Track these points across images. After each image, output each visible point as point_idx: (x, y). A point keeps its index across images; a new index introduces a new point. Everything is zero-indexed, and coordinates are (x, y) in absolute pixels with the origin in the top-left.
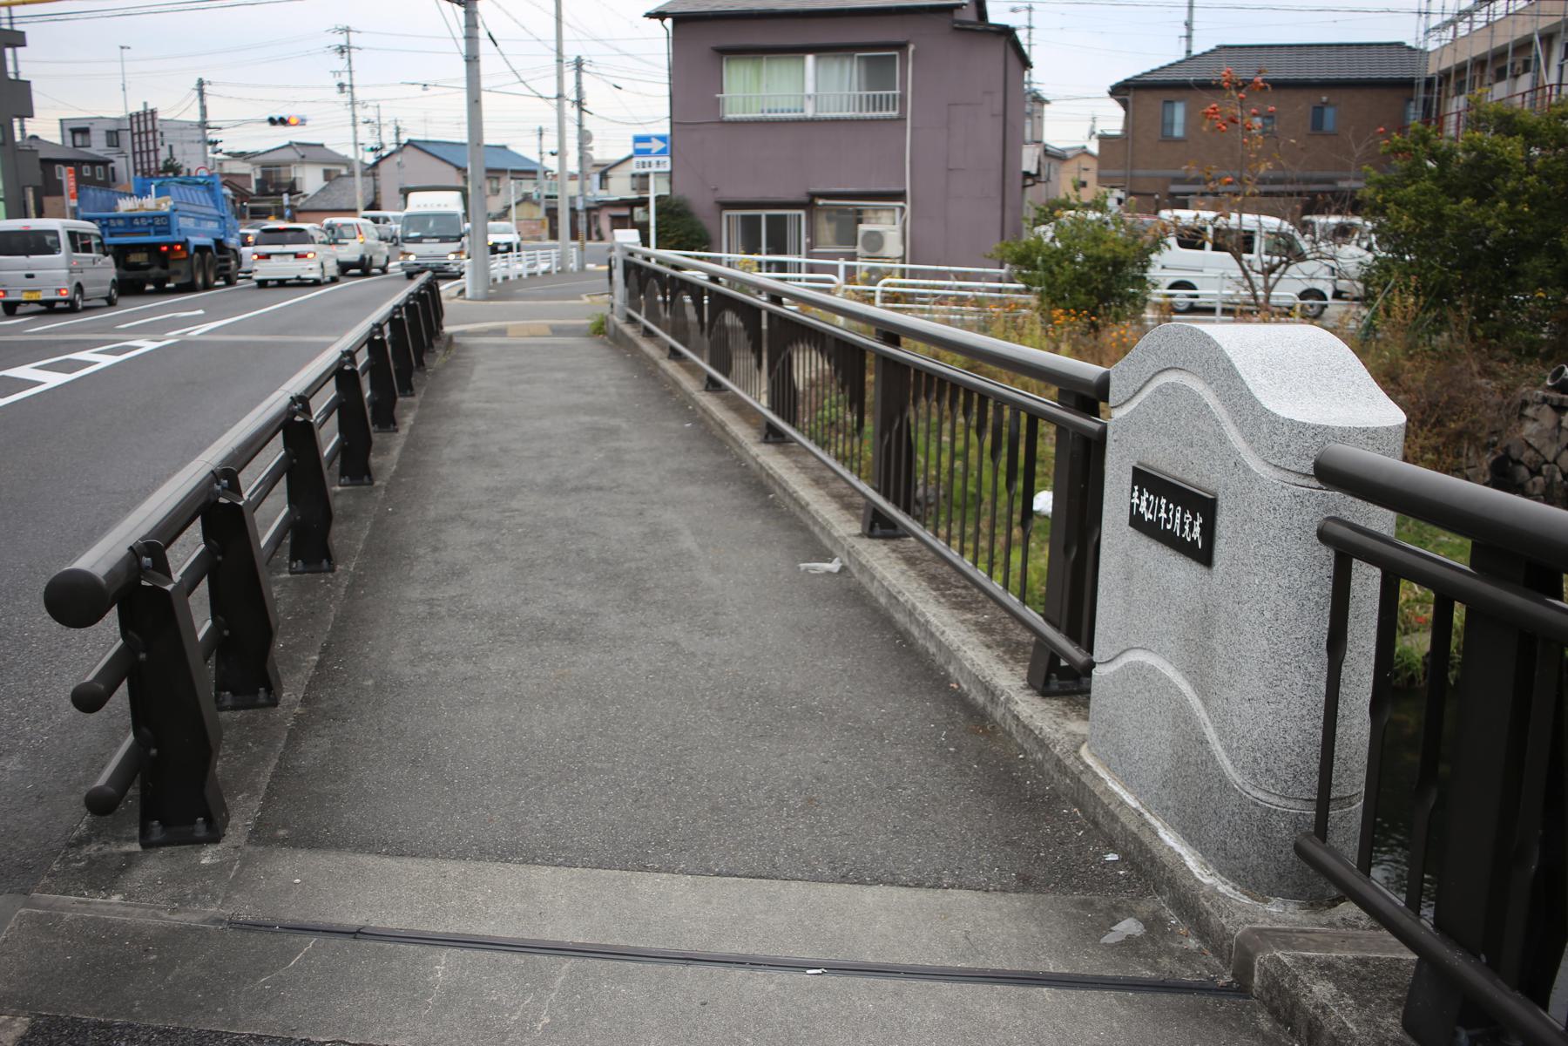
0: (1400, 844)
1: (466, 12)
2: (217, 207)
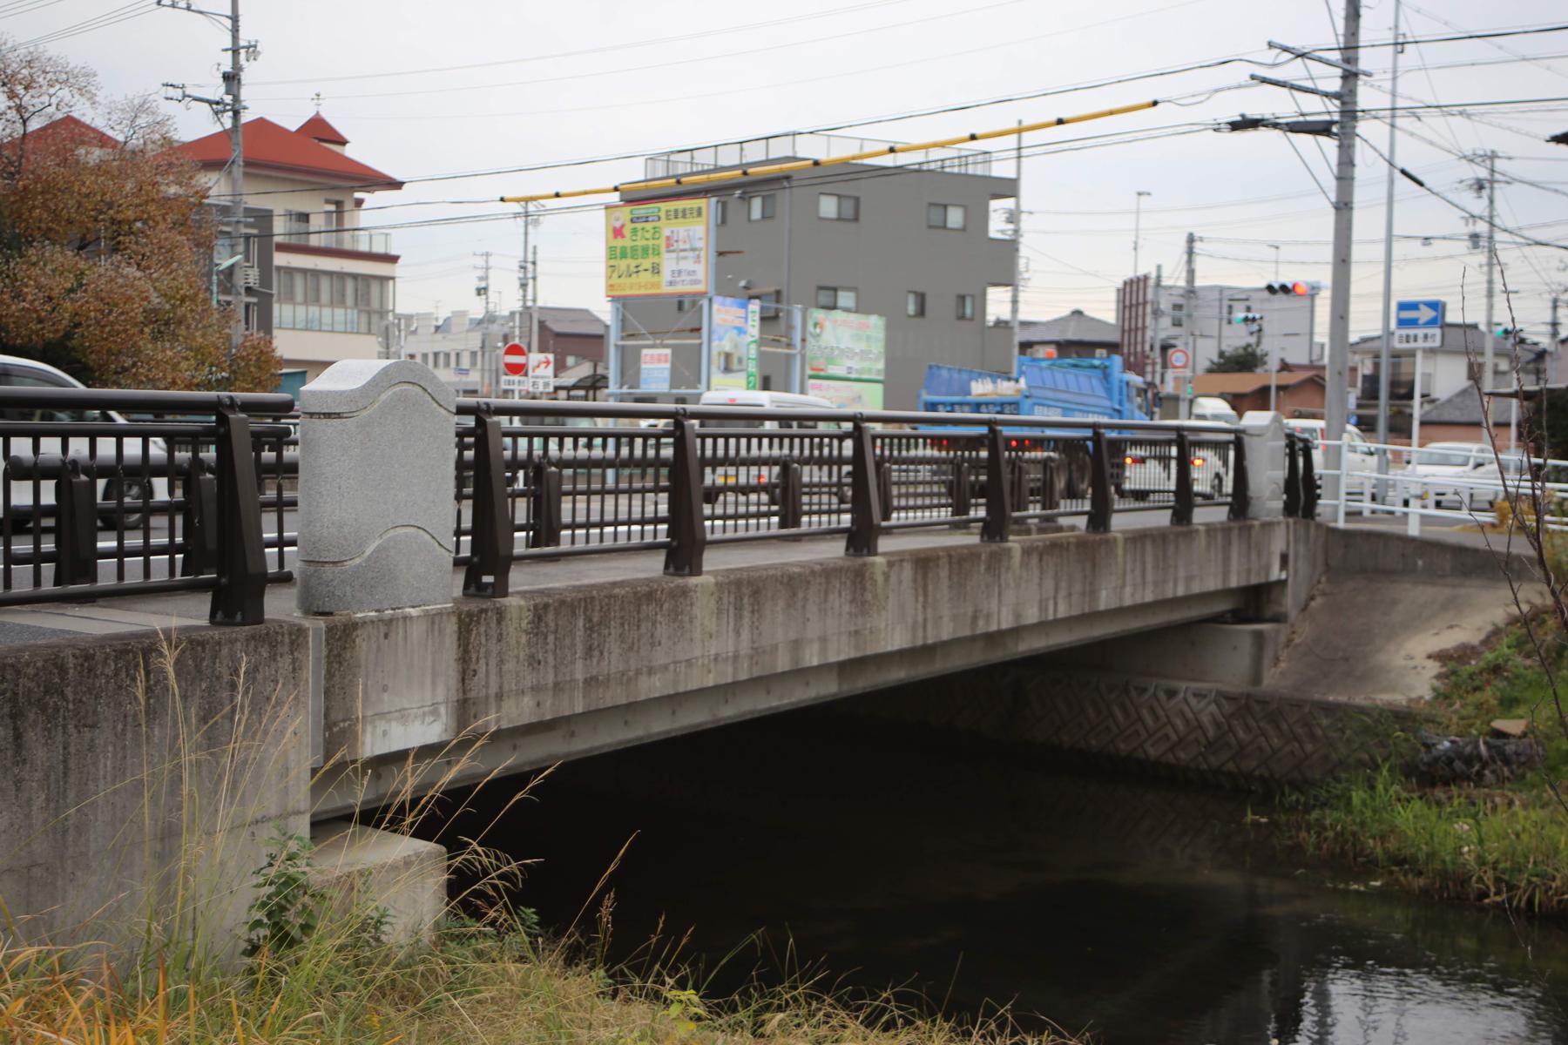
0: (1346, 966)
1: (1340, 147)
2: (1110, 398)
